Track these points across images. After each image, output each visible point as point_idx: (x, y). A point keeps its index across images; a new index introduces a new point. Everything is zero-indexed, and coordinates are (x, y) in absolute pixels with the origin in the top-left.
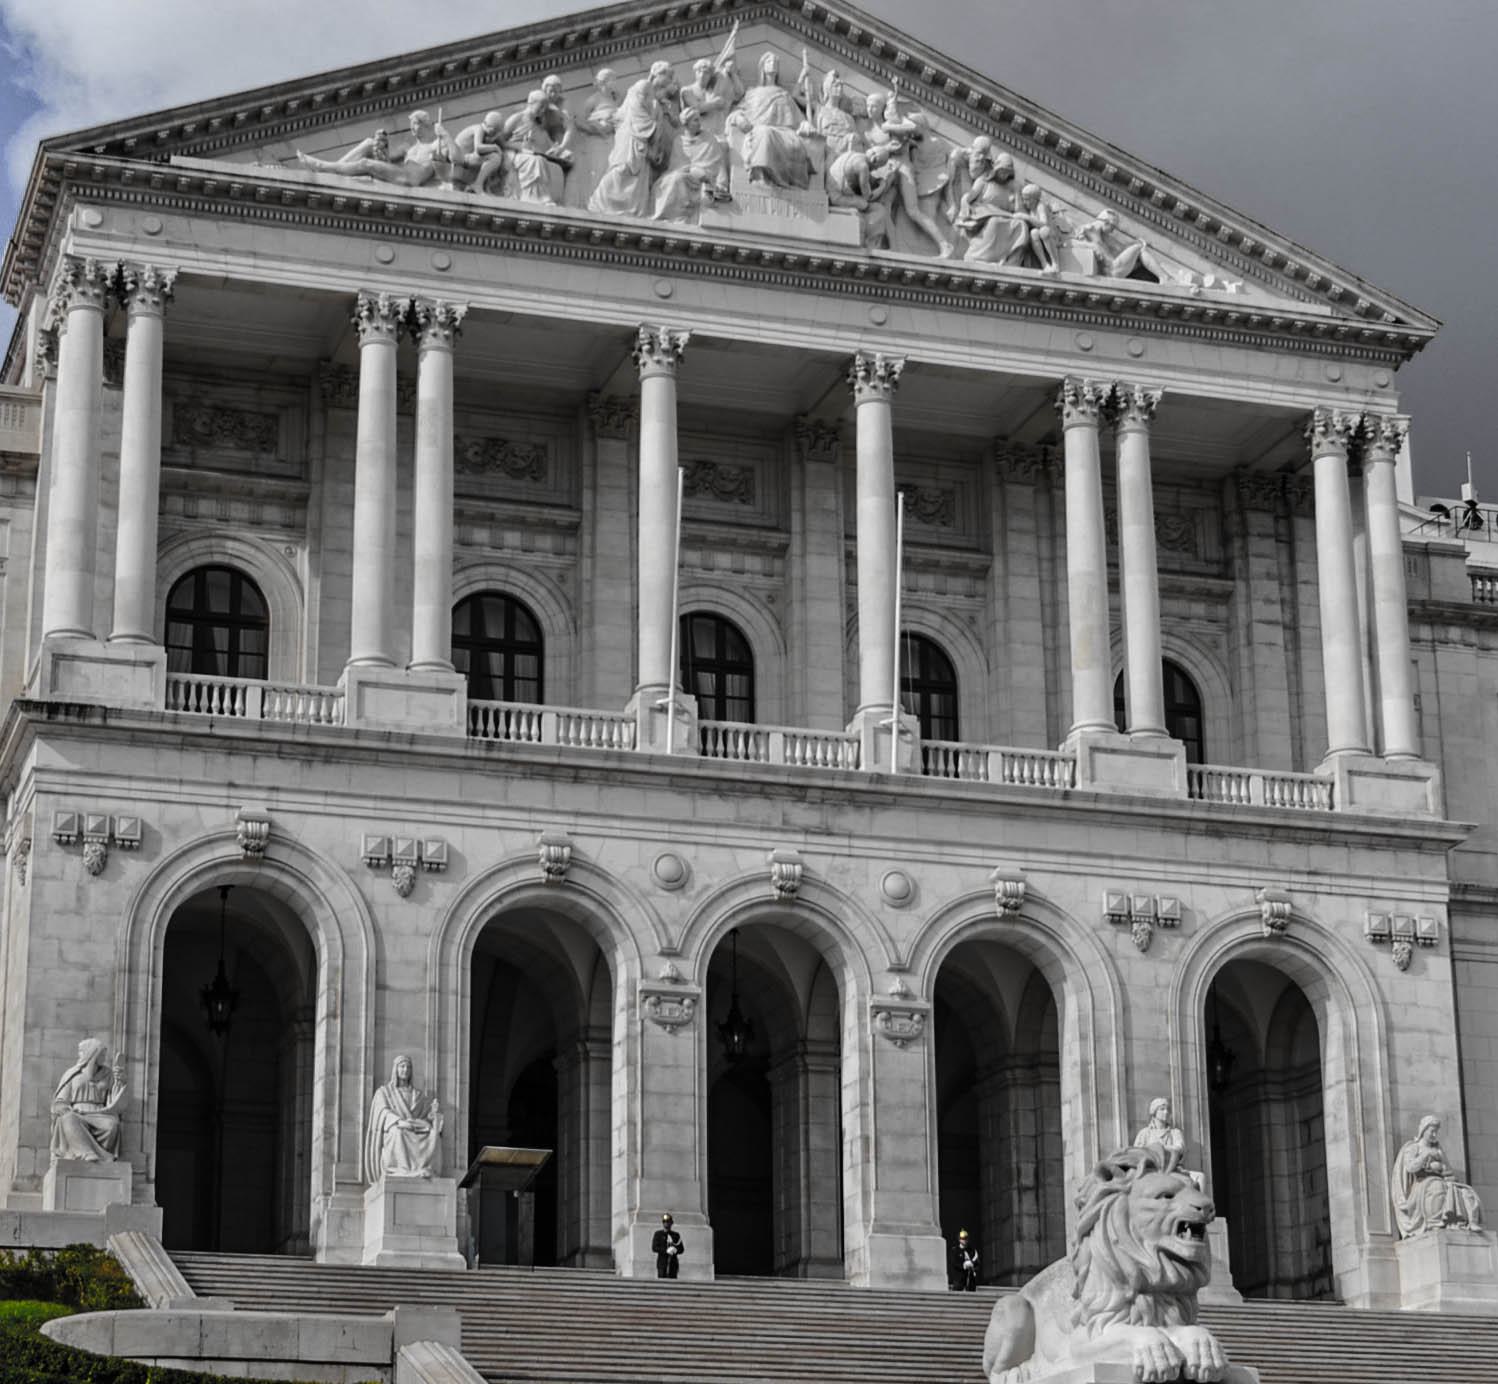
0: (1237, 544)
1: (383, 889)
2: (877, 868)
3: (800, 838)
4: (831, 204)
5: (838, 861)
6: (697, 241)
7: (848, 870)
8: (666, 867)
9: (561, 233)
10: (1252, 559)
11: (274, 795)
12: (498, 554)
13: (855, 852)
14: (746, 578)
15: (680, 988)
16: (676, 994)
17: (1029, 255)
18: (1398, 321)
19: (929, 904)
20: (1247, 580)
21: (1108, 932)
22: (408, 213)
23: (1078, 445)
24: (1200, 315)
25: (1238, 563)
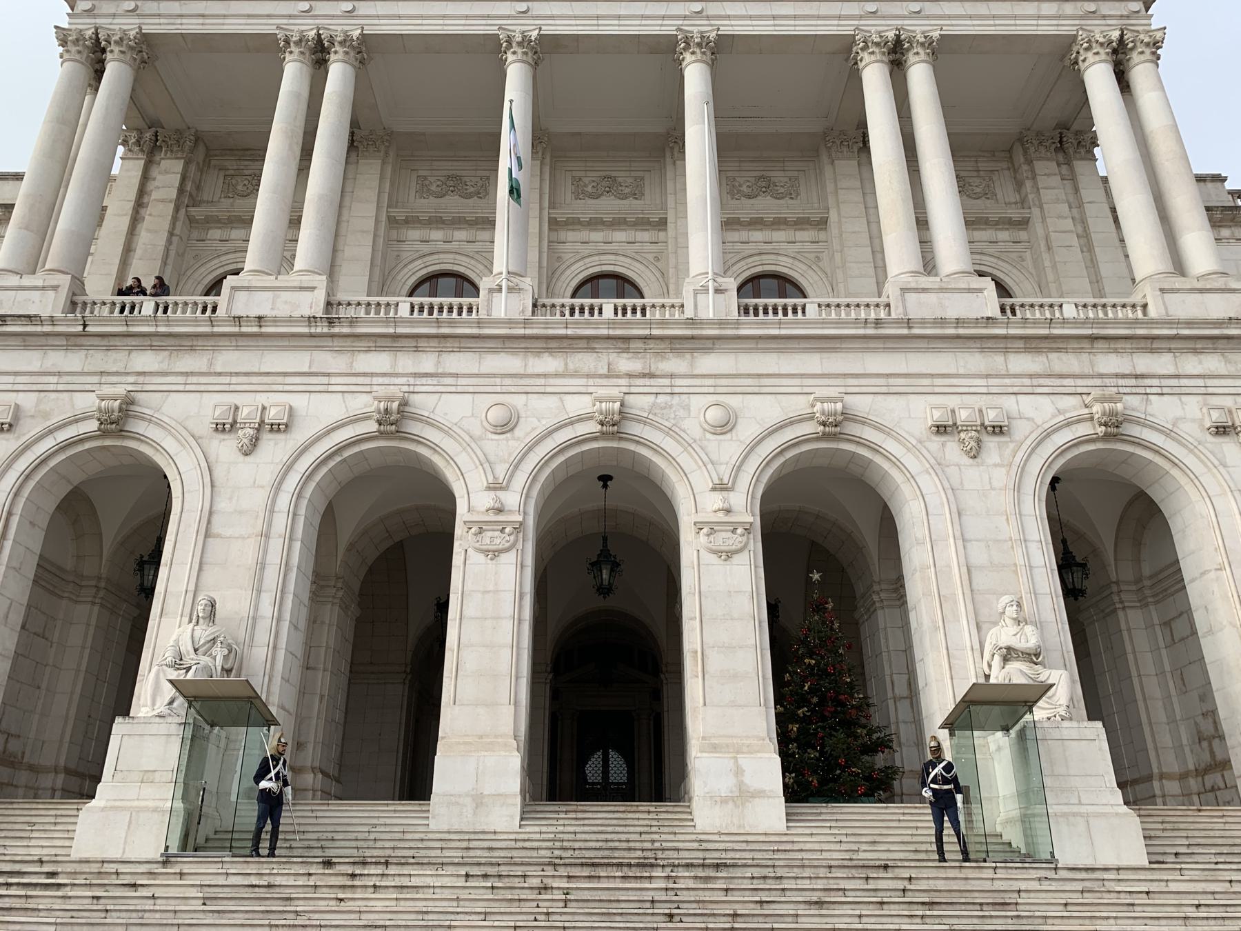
1: (225, 449)
5: (661, 399)
7: (671, 407)
8: (496, 415)
11: (141, 379)
12: (448, 246)
13: (676, 390)
14: (637, 247)
15: (501, 518)
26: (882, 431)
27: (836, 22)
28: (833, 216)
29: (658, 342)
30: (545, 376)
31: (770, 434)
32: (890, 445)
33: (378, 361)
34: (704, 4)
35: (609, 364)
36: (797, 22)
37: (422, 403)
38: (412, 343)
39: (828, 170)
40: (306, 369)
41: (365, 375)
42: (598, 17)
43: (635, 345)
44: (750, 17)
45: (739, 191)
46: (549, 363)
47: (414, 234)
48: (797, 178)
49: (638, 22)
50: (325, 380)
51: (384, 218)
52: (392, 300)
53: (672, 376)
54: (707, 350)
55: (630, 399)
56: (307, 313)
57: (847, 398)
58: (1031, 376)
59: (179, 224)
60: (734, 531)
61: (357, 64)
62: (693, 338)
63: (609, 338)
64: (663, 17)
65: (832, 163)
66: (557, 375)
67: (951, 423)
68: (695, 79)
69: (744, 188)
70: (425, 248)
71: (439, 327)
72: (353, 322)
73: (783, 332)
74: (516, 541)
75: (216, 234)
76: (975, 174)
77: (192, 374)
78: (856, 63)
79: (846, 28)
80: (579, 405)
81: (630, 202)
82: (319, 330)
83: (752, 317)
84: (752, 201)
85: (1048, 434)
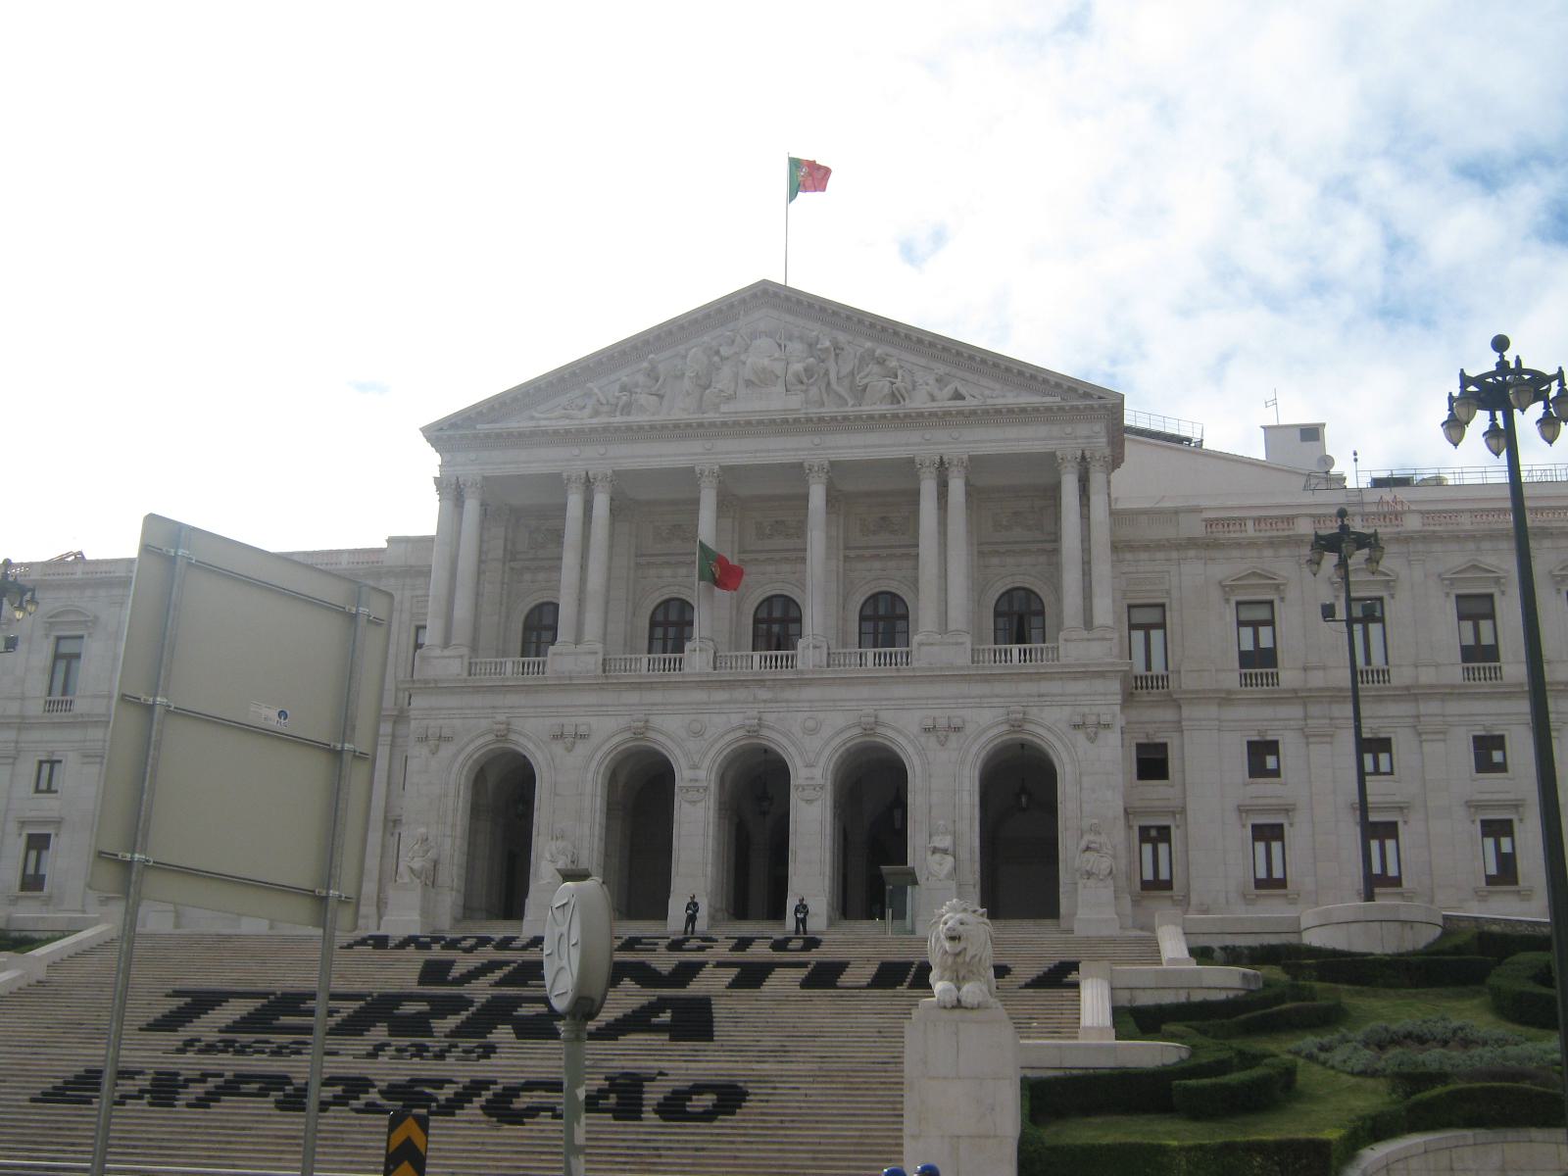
1: (558, 748)
9: (652, 427)
13: (791, 709)
15: (697, 784)
16: (694, 787)
17: (895, 397)
18: (1100, 398)
22: (580, 432)
23: (928, 489)
24: (986, 412)
32: (901, 740)
33: (633, 697)
37: (656, 721)
41: (626, 705)
43: (768, 683)
46: (722, 695)
52: (638, 656)
53: (787, 701)
55: (766, 716)
72: (616, 677)
73: (848, 675)
80: (736, 719)
85: (984, 731)
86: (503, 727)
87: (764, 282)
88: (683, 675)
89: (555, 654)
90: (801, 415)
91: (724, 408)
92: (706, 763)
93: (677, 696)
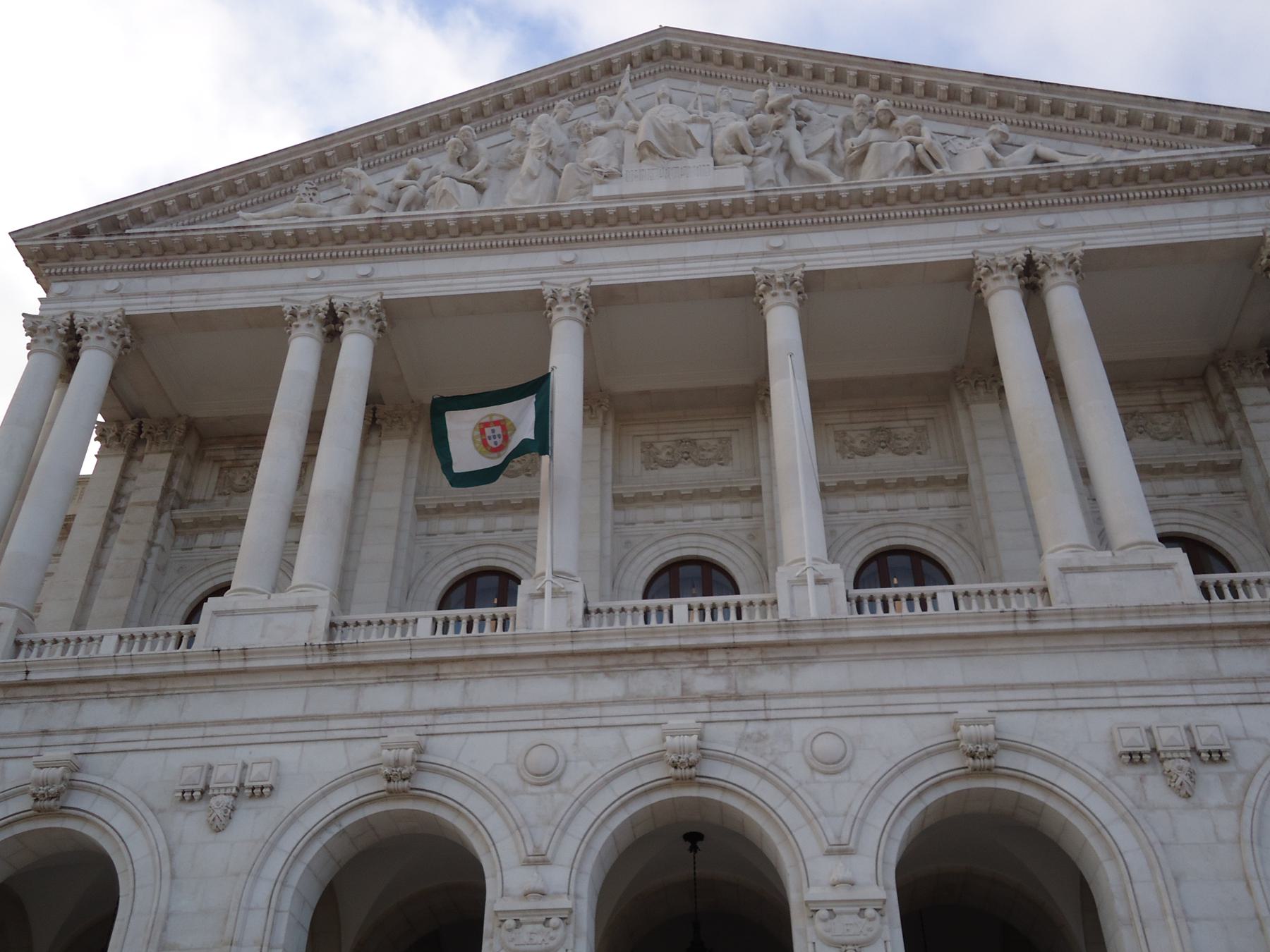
0: (1233, 418)
1: (192, 823)
2: (801, 731)
3: (703, 706)
4: (716, 164)
5: (752, 728)
6: (589, 208)
10: (1252, 426)
11: (92, 737)
13: (773, 714)
15: (545, 904)
17: (919, 166)
19: (869, 767)
20: (1254, 447)
21: (1128, 778)
23: (1007, 312)
25: (1239, 434)
26: (1054, 762)
27: (950, 246)
28: (973, 476)
29: (745, 651)
30: (601, 704)
31: (902, 771)
33: (390, 696)
34: (785, 237)
35: (683, 684)
36: (901, 250)
37: (443, 750)
38: (432, 670)
39: (961, 415)
40: (299, 712)
42: (659, 261)
43: (714, 657)
44: (843, 248)
45: (851, 449)
47: (447, 524)
48: (924, 428)
49: (707, 264)
50: (323, 725)
51: (410, 508)
52: (409, 615)
53: (765, 696)
54: (807, 660)
56: (301, 638)
57: (1001, 718)
58: (1255, 680)
59: (161, 532)
60: (861, 912)
61: (375, 334)
62: (789, 645)
63: (681, 649)
64: (737, 256)
65: (967, 407)
66: (615, 702)
67: (1148, 749)
68: (782, 326)
69: (858, 445)
70: (461, 541)
71: (465, 648)
72: (358, 648)
74: (565, 938)
75: (205, 539)
76: (1158, 409)
77: (158, 727)
78: (979, 291)
79: (959, 252)
80: (641, 741)
81: (715, 469)
82: (317, 661)
83: (867, 613)
84: (866, 460)
86: (55, 773)
87: (663, 30)
88: (515, 640)
89: (217, 613)
90: (748, 196)
91: (598, 191)
92: (568, 849)
93: (489, 691)
